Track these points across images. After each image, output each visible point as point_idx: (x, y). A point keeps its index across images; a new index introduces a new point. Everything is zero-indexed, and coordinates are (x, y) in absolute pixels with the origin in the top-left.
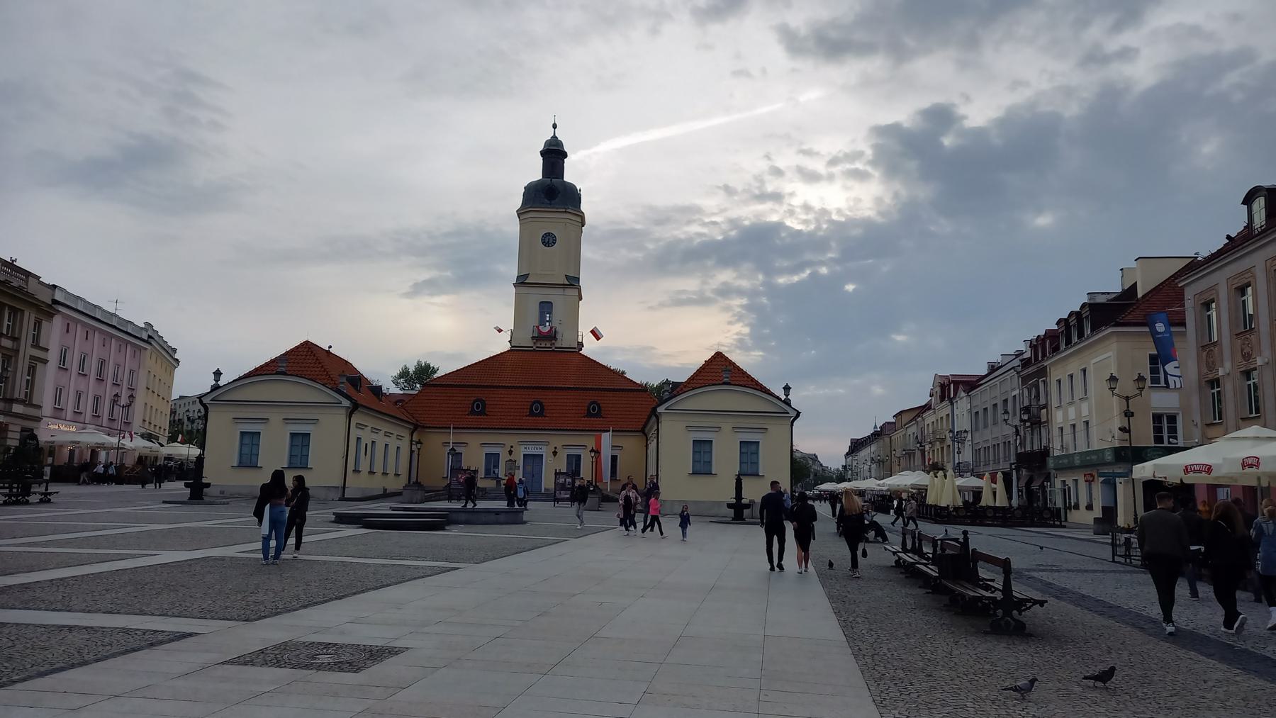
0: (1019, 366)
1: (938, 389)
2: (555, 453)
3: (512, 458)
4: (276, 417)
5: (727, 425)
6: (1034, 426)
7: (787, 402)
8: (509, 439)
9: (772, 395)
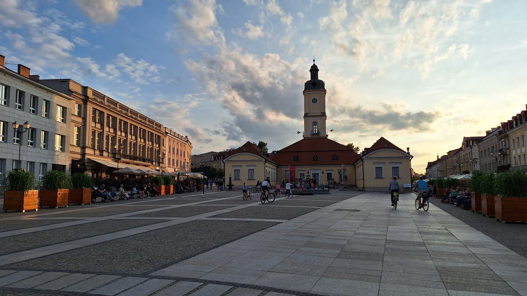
0: (498, 134)
1: (465, 142)
2: (323, 173)
3: (309, 175)
4: (244, 165)
5: (387, 161)
6: (504, 156)
7: (408, 153)
8: (307, 169)
9: (403, 151)
